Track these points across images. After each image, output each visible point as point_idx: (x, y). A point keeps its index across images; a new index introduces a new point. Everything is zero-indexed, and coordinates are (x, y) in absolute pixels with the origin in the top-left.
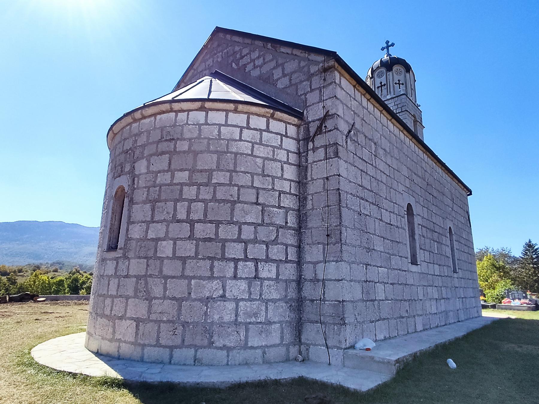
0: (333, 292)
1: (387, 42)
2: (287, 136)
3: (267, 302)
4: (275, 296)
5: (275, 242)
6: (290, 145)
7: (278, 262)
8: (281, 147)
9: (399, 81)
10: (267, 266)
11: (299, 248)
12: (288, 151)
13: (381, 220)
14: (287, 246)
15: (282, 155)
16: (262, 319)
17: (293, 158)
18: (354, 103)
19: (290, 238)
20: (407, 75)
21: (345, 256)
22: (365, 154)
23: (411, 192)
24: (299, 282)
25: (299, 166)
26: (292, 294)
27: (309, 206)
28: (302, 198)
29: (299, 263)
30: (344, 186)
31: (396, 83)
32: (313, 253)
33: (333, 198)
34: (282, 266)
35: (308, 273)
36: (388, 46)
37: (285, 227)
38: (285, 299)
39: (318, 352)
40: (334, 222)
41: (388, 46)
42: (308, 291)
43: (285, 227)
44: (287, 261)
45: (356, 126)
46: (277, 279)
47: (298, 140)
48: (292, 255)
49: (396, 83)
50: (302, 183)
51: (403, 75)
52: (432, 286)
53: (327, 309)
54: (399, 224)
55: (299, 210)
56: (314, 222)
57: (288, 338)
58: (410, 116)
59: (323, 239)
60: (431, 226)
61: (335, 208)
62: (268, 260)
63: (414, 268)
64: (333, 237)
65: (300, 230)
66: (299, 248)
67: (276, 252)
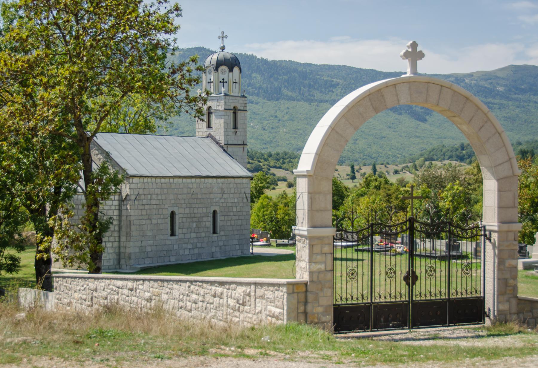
0: (128, 251)
1: (223, 33)
2: (115, 200)
3: (109, 253)
4: (111, 251)
5: (111, 236)
6: (116, 203)
7: (112, 242)
8: (112, 205)
9: (223, 79)
10: (109, 243)
11: (119, 237)
12: (115, 206)
13: (152, 224)
14: (115, 237)
15: (113, 208)
16: (108, 258)
17: (117, 207)
18: (139, 185)
19: (116, 234)
20: (231, 74)
21: (132, 240)
22: (144, 202)
23: (175, 205)
24: (119, 247)
25: (119, 210)
26: (117, 251)
27: (122, 224)
28: (120, 221)
29: (119, 241)
30: (132, 218)
31: (220, 82)
32: (123, 239)
33: (128, 223)
34: (114, 243)
35: (122, 245)
36: (223, 37)
37: (115, 231)
38: (115, 252)
39: (124, 267)
40: (128, 230)
41: (223, 37)
42: (122, 250)
43: (115, 231)
44: (115, 241)
45: (140, 193)
46: (112, 247)
47: (119, 200)
48: (117, 239)
49: (220, 82)
50: (120, 215)
51: (227, 74)
52: (187, 243)
53: (127, 255)
54: (163, 222)
55: (119, 225)
56: (124, 229)
57: (116, 263)
58: (228, 111)
59: (125, 235)
60: (193, 215)
61: (129, 226)
62: (109, 241)
63: (173, 238)
64: (128, 234)
65: (119, 231)
66: (119, 237)
67: (112, 239)
